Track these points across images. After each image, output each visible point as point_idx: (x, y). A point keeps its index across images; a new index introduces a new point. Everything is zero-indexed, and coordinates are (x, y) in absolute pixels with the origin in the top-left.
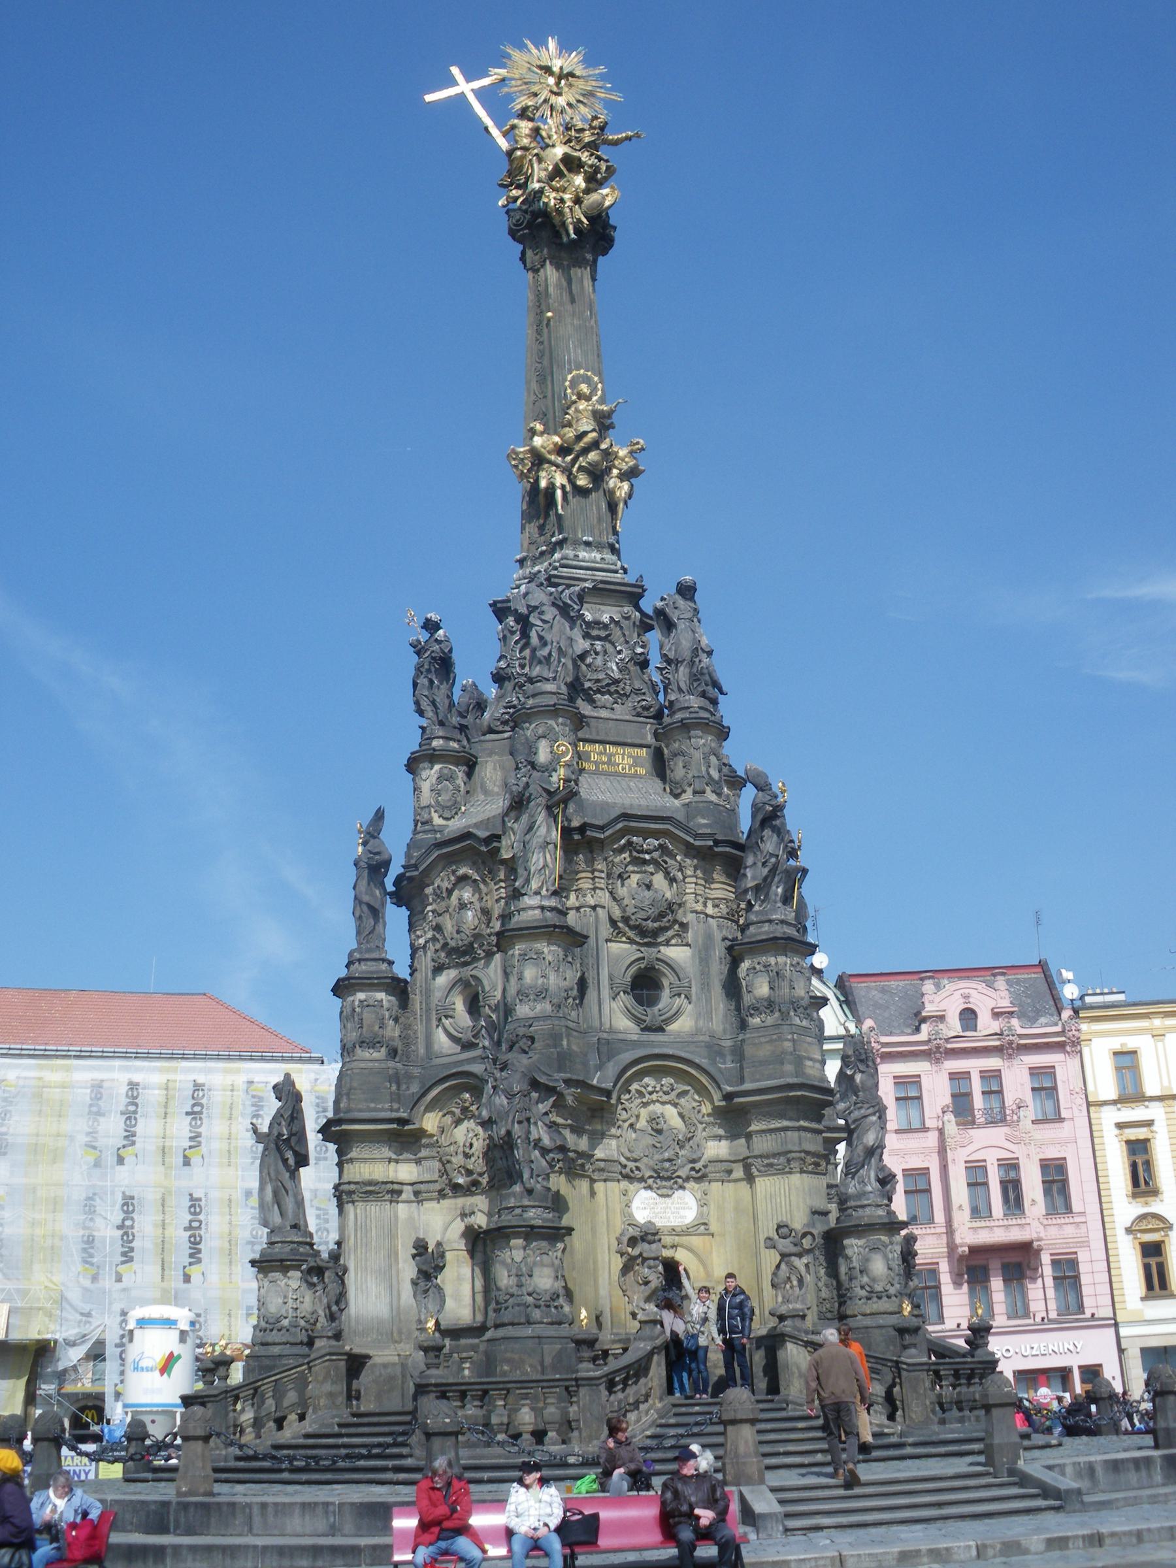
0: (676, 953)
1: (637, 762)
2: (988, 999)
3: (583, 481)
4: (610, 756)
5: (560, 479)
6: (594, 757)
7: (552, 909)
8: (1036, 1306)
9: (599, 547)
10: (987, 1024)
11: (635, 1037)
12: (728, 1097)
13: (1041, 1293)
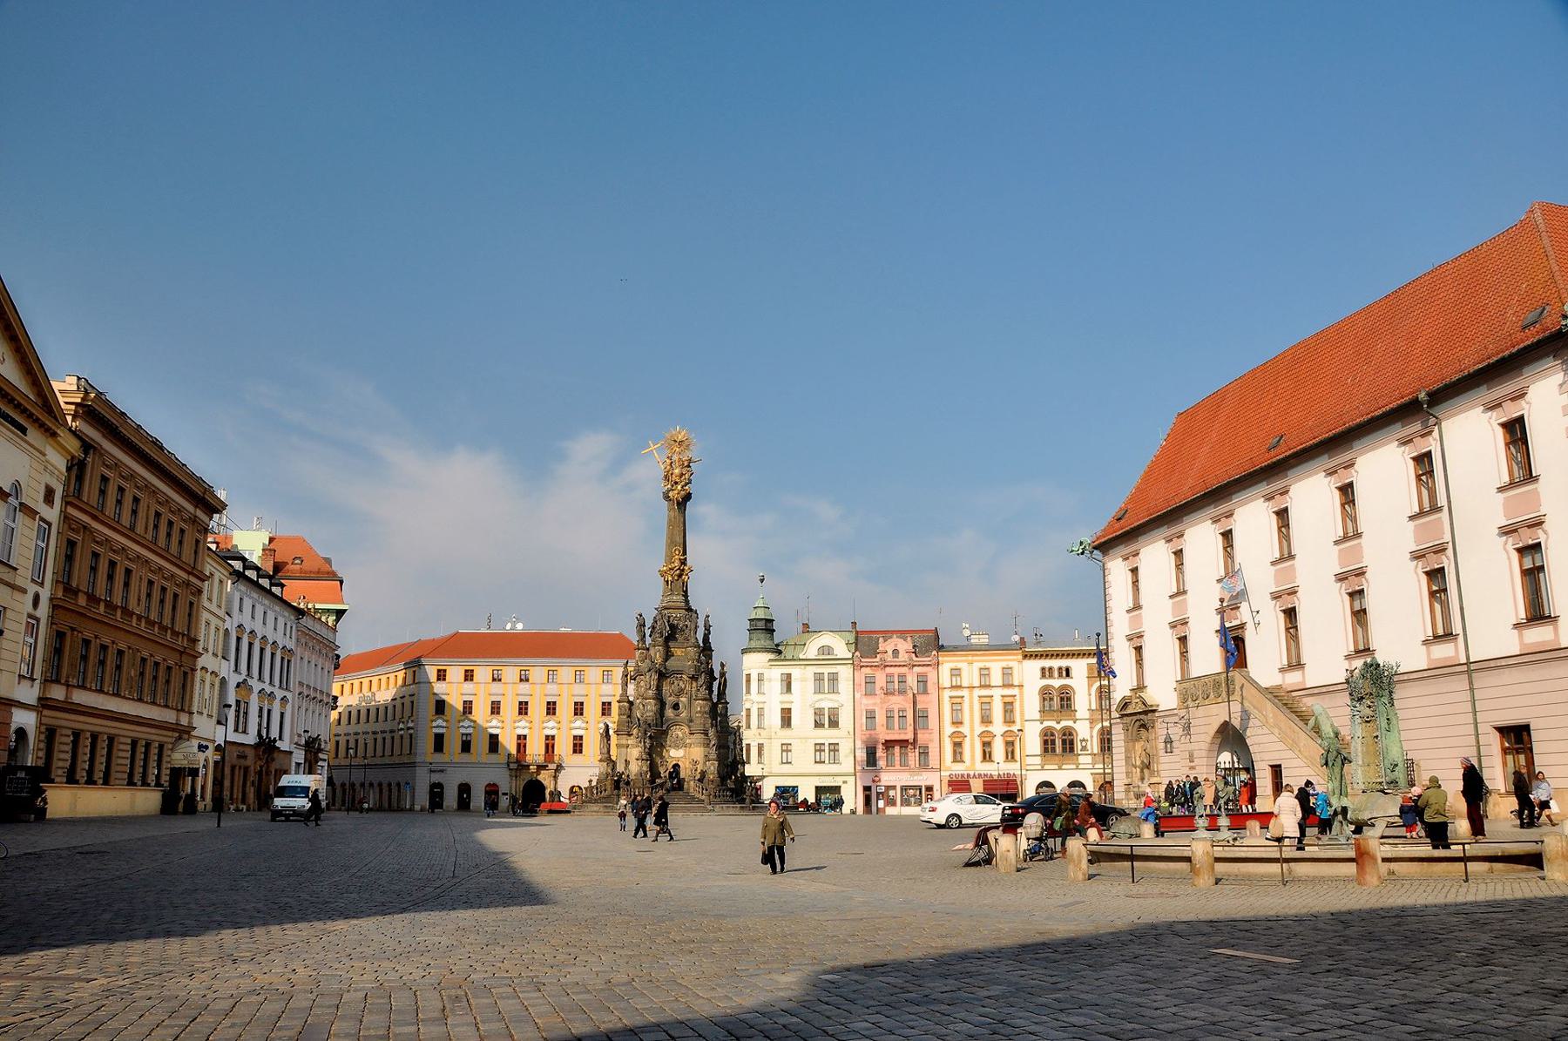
2: (904, 646)
8: (911, 763)
10: (903, 657)
13: (913, 757)
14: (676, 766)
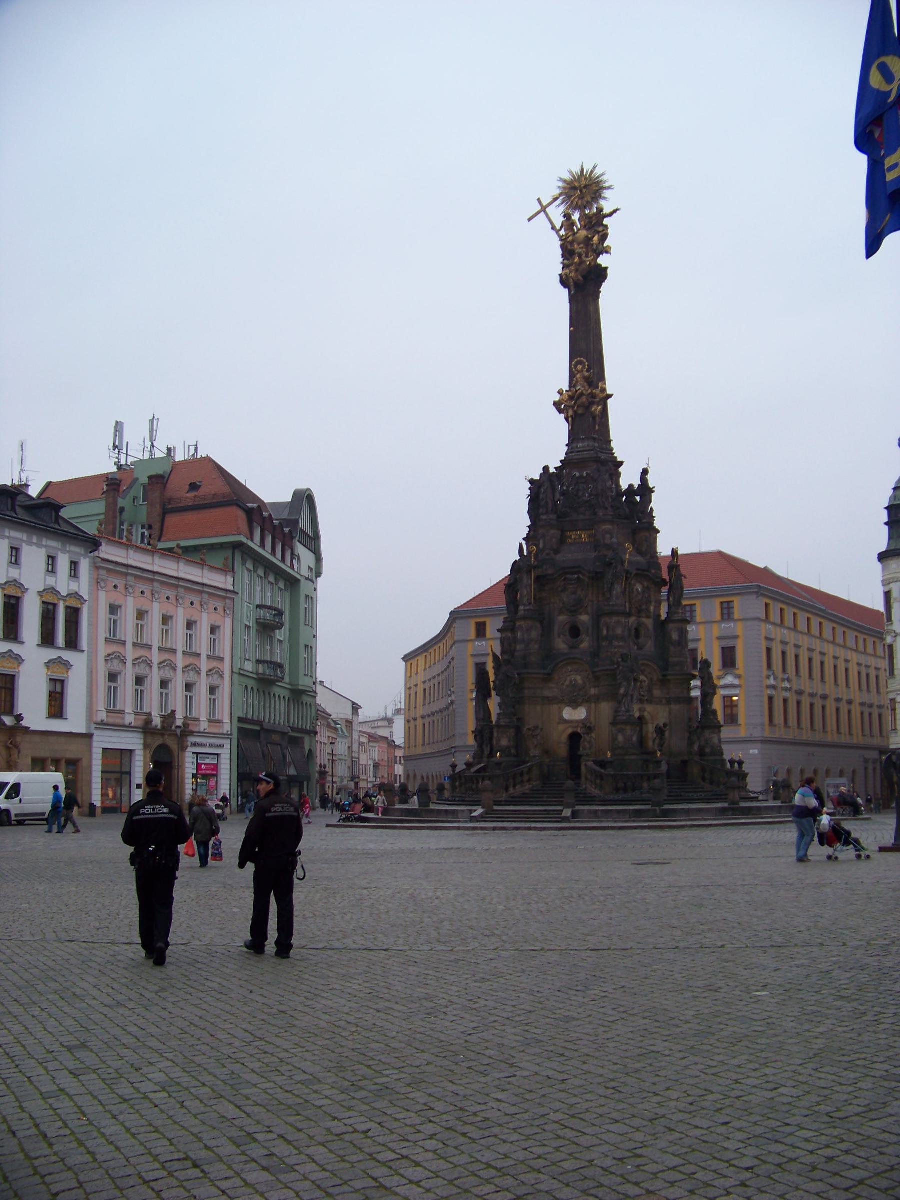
0: (585, 618)
1: (590, 537)
3: (580, 412)
4: (580, 536)
5: (571, 413)
6: (574, 537)
7: (528, 610)
9: (587, 439)
11: (566, 652)
12: (593, 673)
14: (575, 739)
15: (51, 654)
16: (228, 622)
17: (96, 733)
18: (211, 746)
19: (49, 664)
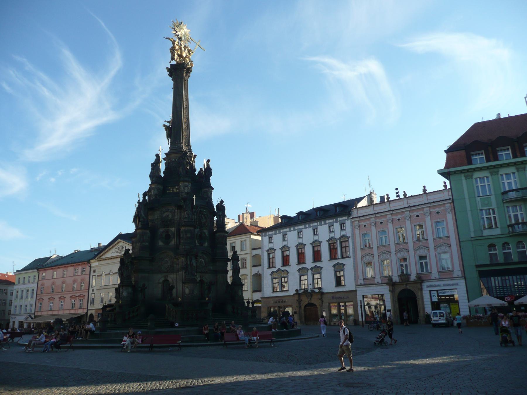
15: (336, 262)
16: (450, 217)
17: (357, 289)
18: (444, 285)
19: (334, 266)
